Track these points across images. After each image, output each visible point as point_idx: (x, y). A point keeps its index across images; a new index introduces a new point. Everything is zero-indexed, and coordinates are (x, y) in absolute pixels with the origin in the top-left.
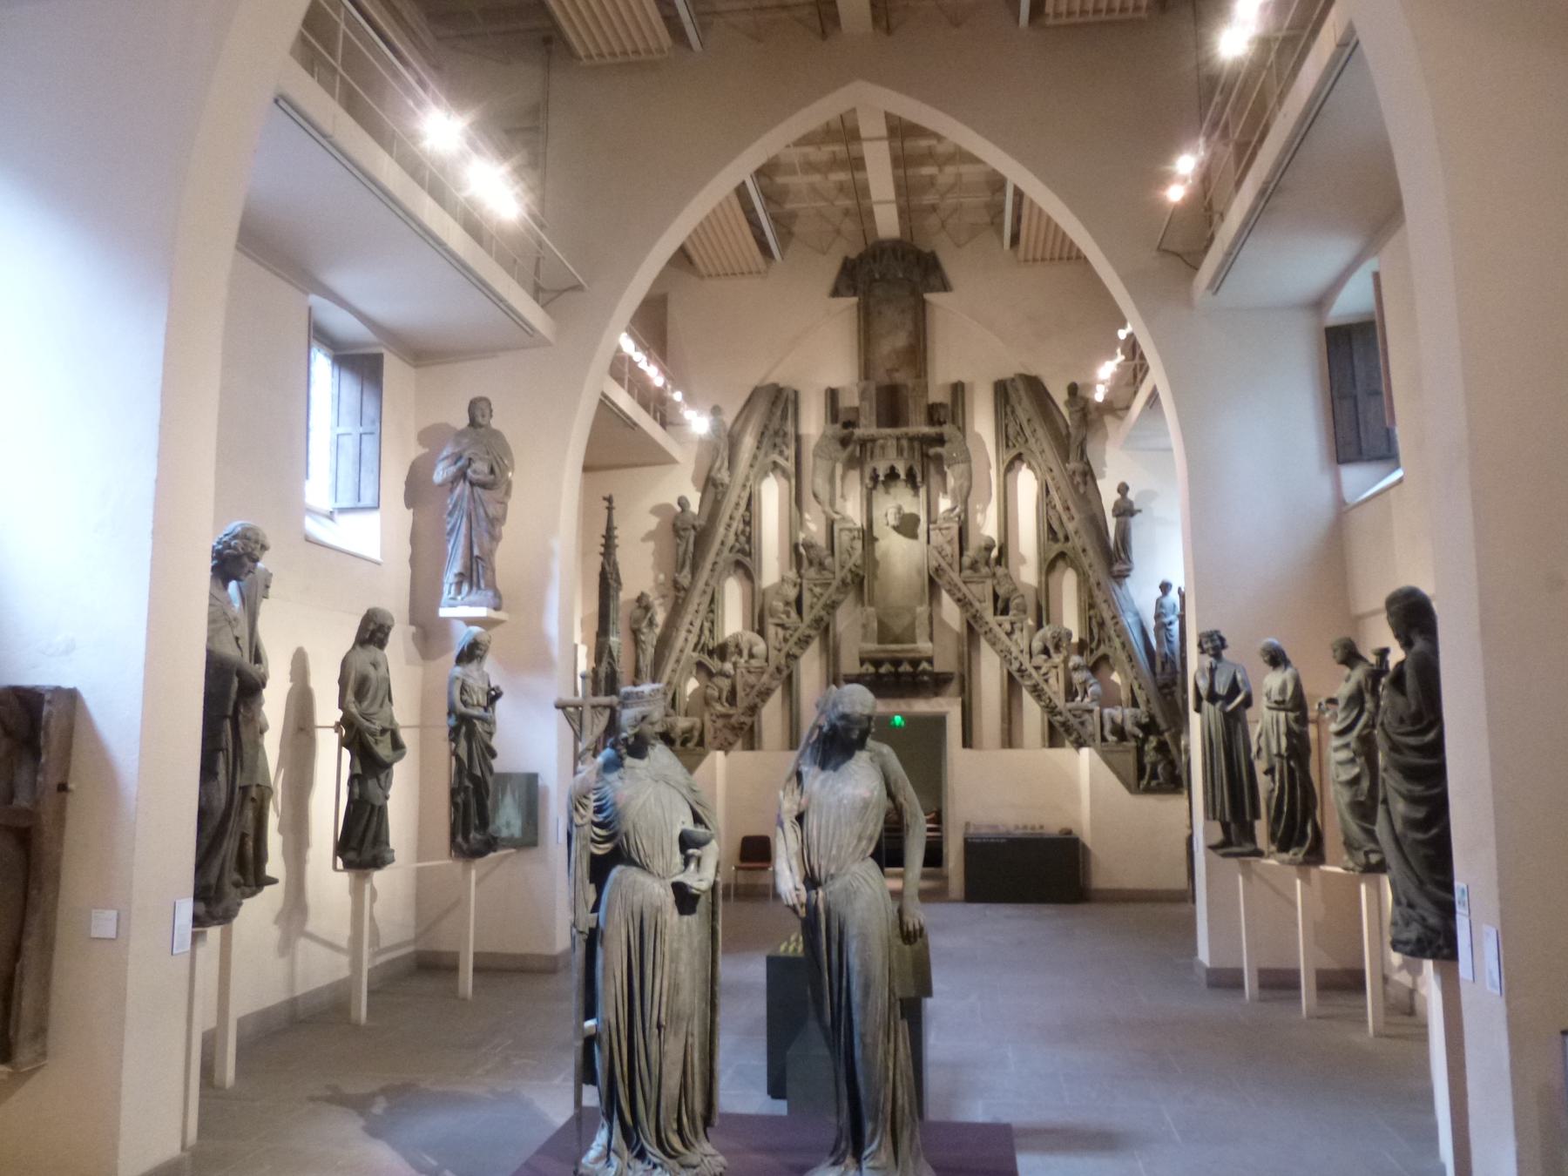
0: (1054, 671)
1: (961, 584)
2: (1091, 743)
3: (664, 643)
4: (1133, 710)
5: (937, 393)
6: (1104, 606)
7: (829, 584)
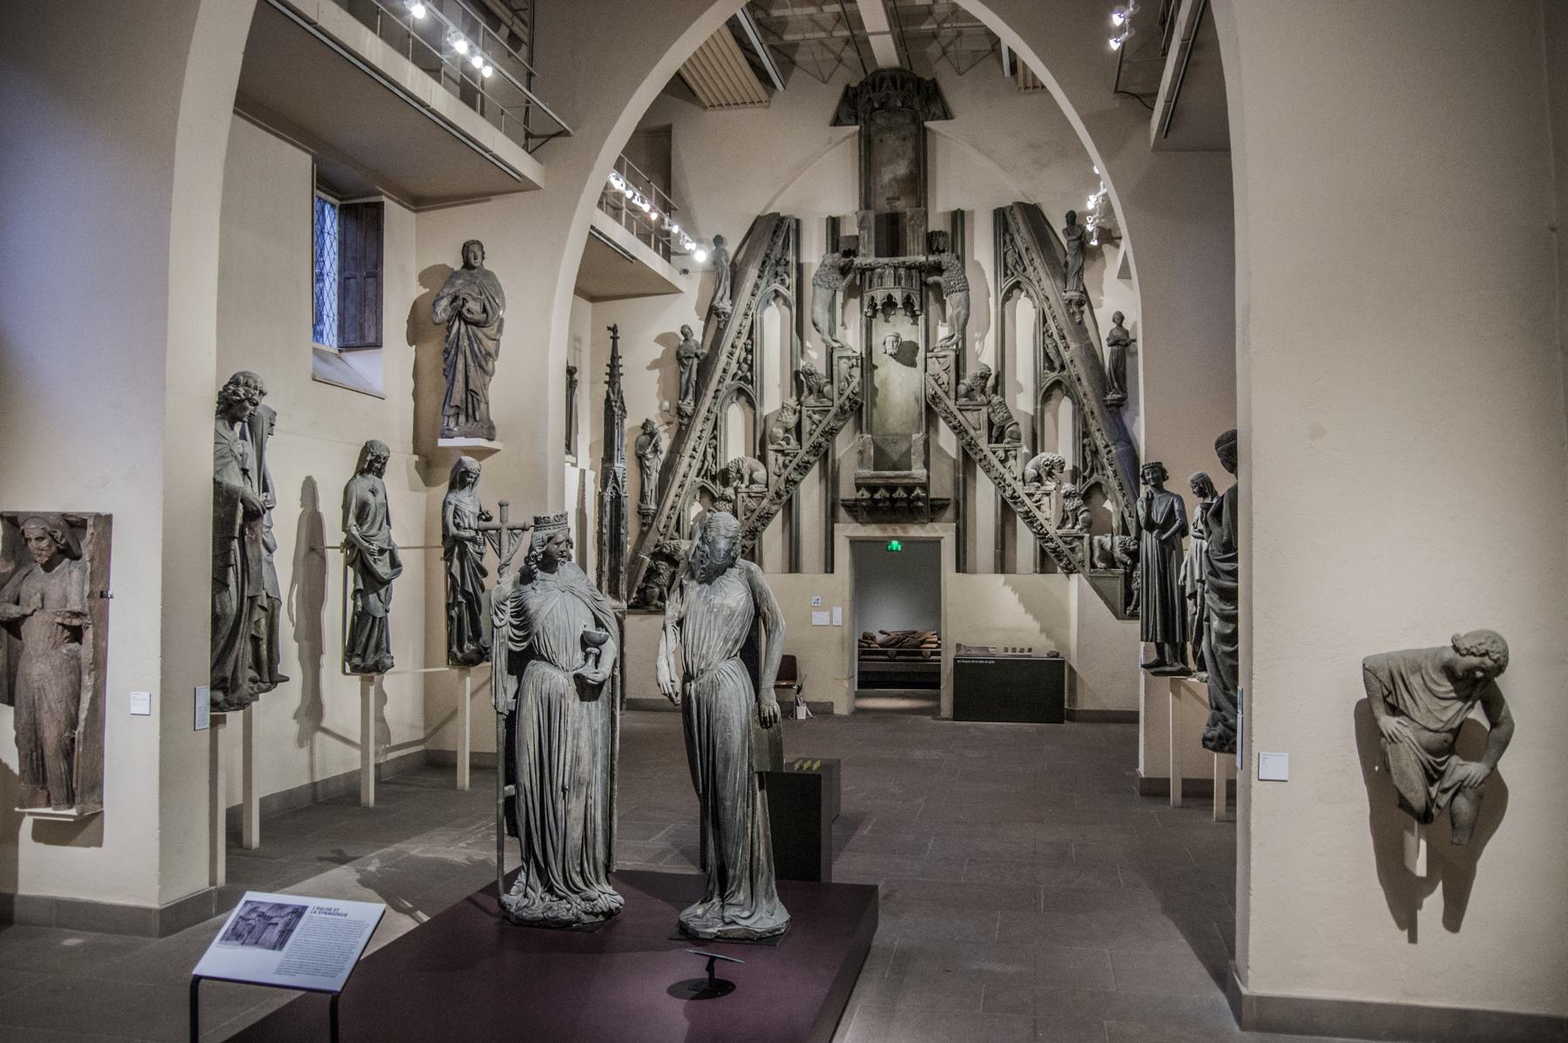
0: (1046, 499)
1: (957, 413)
2: (1081, 569)
3: (668, 468)
5: (937, 223)
7: (829, 411)
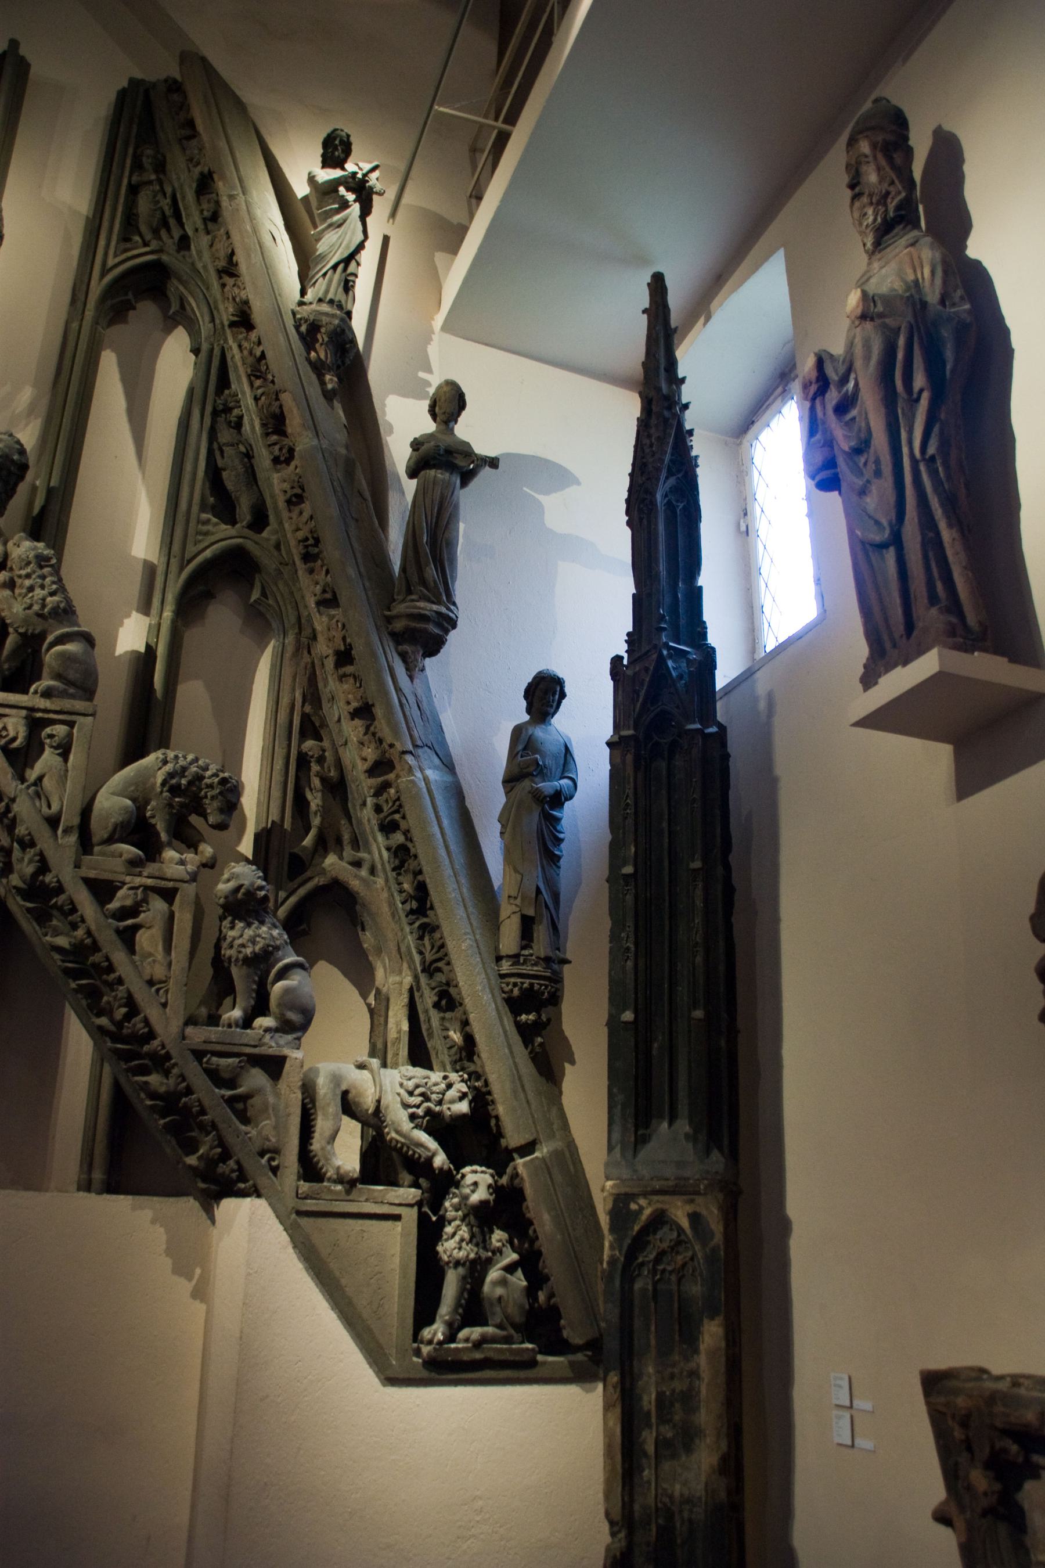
4: (419, 1072)
6: (352, 730)
